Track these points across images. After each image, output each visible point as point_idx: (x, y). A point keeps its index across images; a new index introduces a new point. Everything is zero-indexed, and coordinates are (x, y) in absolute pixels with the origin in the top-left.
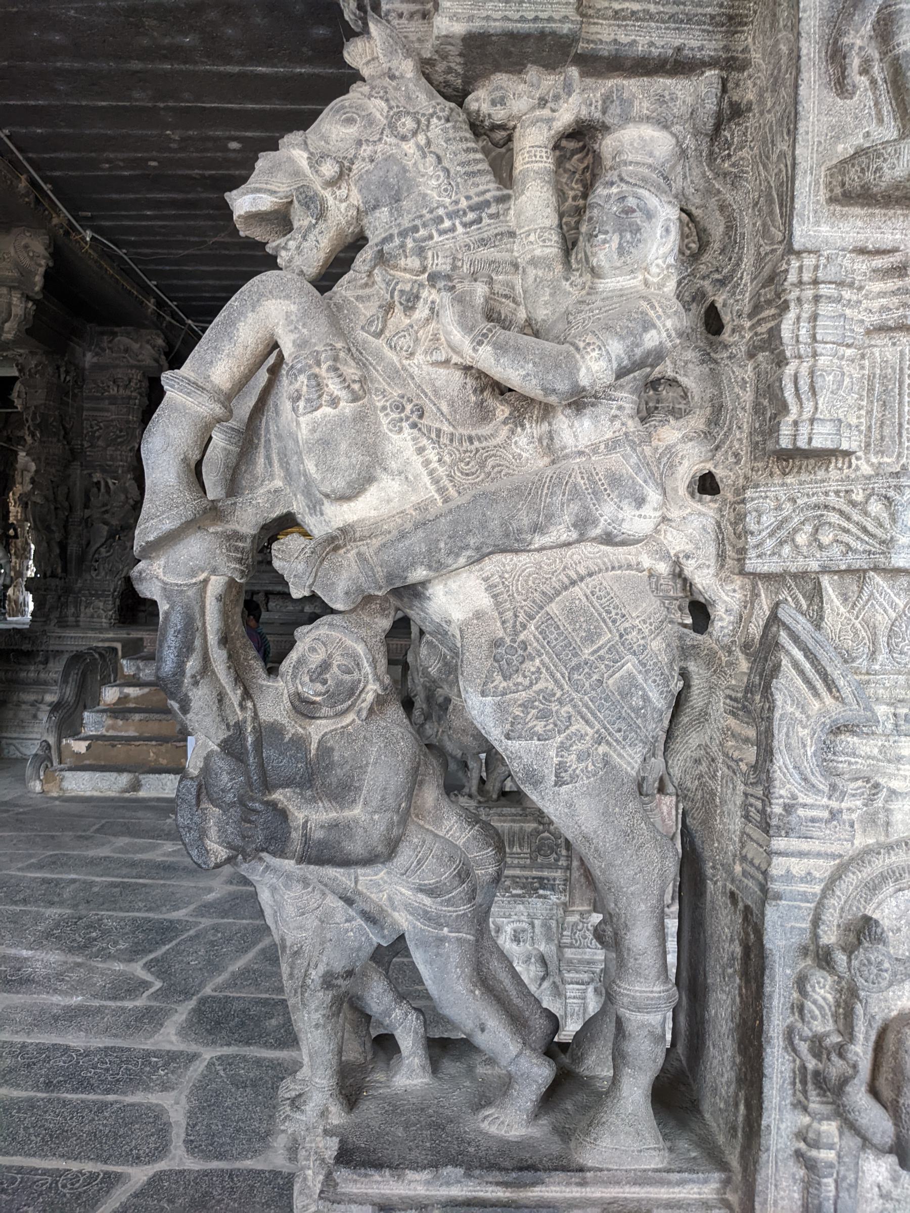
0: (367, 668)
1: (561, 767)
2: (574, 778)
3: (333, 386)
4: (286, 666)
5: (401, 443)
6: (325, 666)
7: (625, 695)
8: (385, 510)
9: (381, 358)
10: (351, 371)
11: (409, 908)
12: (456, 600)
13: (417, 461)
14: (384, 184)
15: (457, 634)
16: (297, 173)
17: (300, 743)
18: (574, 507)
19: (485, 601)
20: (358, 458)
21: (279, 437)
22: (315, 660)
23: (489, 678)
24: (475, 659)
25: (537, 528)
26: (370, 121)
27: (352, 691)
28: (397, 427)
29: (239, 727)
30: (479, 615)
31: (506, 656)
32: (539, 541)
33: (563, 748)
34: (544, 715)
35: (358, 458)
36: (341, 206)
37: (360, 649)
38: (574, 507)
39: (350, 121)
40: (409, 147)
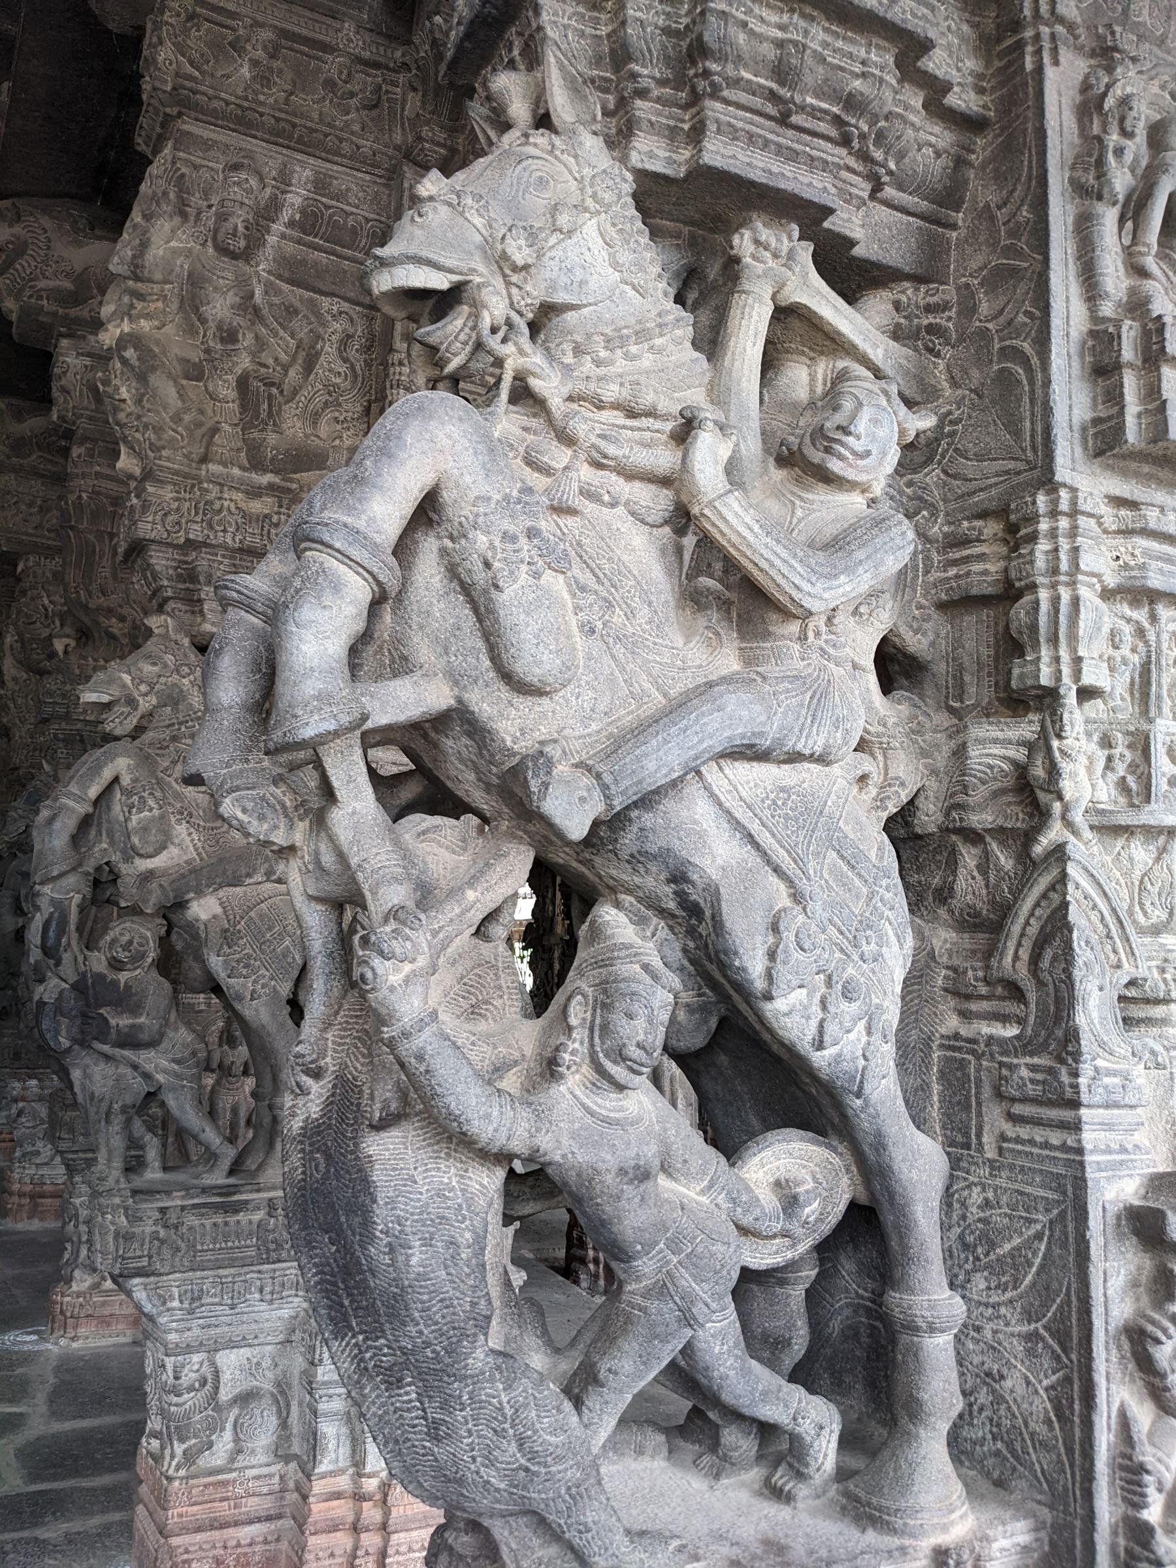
0: (151, 944)
1: (254, 991)
2: (259, 997)
3: (151, 802)
4: (101, 943)
5: (181, 830)
6: (130, 942)
7: (285, 956)
8: (170, 863)
9: (171, 787)
10: (158, 794)
11: (165, 1071)
12: (204, 909)
13: (188, 839)
14: (170, 696)
15: (202, 927)
16: (124, 686)
17: (115, 983)
18: (266, 865)
19: (219, 910)
20: (161, 837)
21: (109, 822)
22: (125, 939)
23: (221, 947)
24: (215, 938)
25: (249, 875)
26: (166, 666)
27: (143, 956)
28: (179, 822)
29: (83, 975)
30: (215, 917)
31: (229, 937)
32: (248, 881)
33: (255, 982)
34: (246, 966)
35: (161, 837)
36: (145, 705)
37: (149, 934)
38: (266, 865)
39: (155, 664)
40: (185, 681)
